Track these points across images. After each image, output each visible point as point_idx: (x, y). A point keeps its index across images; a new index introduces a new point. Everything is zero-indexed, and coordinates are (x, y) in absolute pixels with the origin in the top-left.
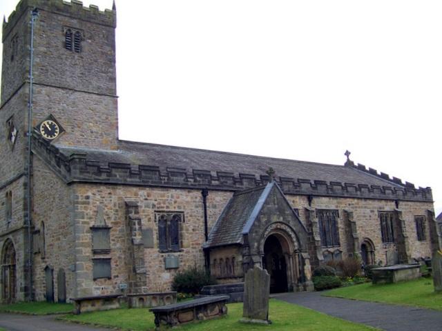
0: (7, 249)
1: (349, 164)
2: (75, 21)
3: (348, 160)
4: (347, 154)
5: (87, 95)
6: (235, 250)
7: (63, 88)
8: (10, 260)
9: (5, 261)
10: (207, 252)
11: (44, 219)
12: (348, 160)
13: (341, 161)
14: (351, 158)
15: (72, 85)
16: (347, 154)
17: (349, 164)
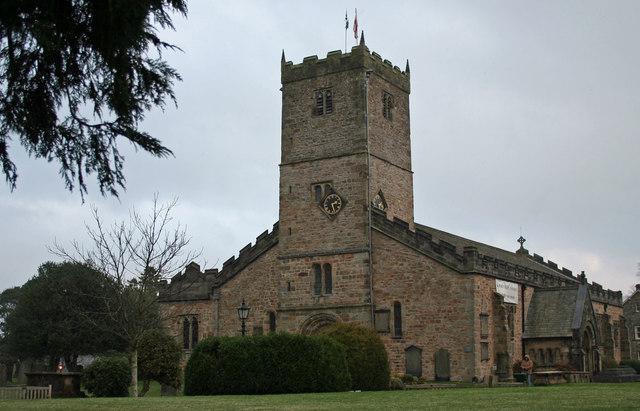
0: (308, 324)
1: (522, 252)
2: (387, 85)
3: (522, 247)
4: (521, 240)
5: (396, 169)
6: (560, 342)
7: (385, 161)
10: (524, 340)
11: (400, 300)
12: (522, 247)
13: (514, 248)
14: (525, 246)
15: (389, 157)
16: (521, 240)
17: (522, 252)
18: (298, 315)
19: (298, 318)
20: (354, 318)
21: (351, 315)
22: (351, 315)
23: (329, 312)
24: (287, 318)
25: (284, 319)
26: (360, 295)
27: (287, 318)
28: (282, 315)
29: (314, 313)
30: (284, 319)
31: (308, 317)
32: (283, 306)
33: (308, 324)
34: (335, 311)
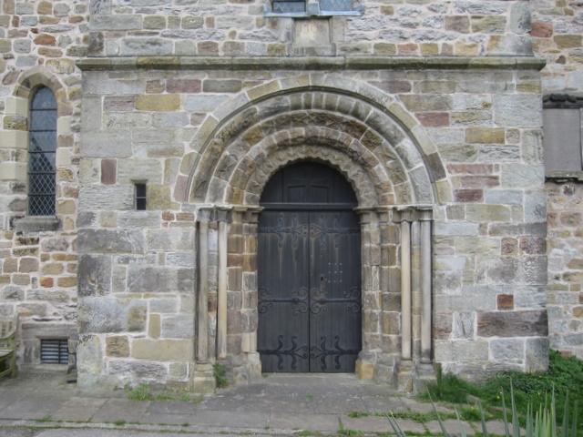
0: (233, 135)
8: (226, 186)
9: (201, 188)
18: (193, 87)
19: (190, 101)
20: (469, 116)
21: (459, 101)
22: (459, 101)
23: (356, 82)
24: (132, 101)
25: (115, 102)
26: (495, 25)
27: (132, 101)
28: (108, 86)
29: (279, 82)
30: (115, 102)
31: (244, 96)
32: (115, 48)
33: (233, 135)
34: (380, 76)
